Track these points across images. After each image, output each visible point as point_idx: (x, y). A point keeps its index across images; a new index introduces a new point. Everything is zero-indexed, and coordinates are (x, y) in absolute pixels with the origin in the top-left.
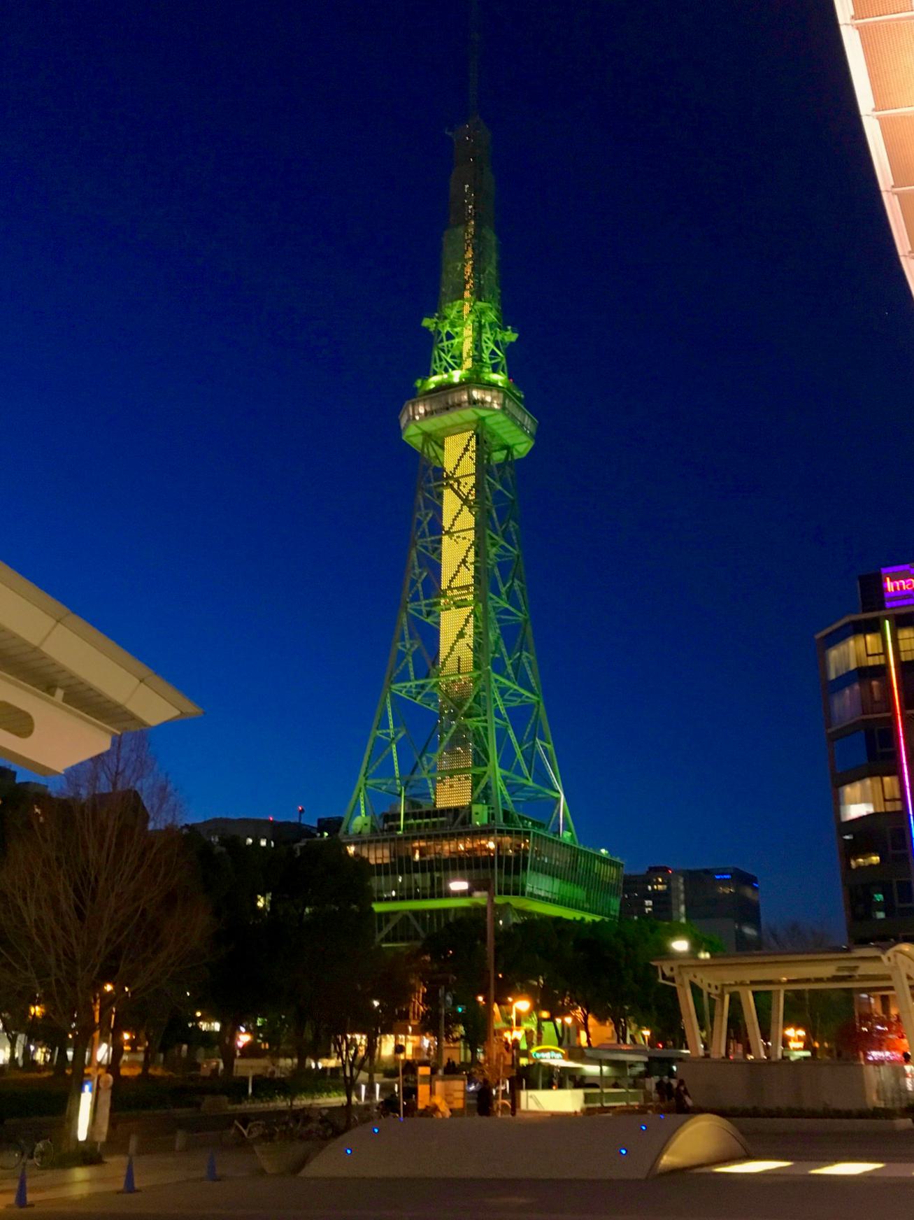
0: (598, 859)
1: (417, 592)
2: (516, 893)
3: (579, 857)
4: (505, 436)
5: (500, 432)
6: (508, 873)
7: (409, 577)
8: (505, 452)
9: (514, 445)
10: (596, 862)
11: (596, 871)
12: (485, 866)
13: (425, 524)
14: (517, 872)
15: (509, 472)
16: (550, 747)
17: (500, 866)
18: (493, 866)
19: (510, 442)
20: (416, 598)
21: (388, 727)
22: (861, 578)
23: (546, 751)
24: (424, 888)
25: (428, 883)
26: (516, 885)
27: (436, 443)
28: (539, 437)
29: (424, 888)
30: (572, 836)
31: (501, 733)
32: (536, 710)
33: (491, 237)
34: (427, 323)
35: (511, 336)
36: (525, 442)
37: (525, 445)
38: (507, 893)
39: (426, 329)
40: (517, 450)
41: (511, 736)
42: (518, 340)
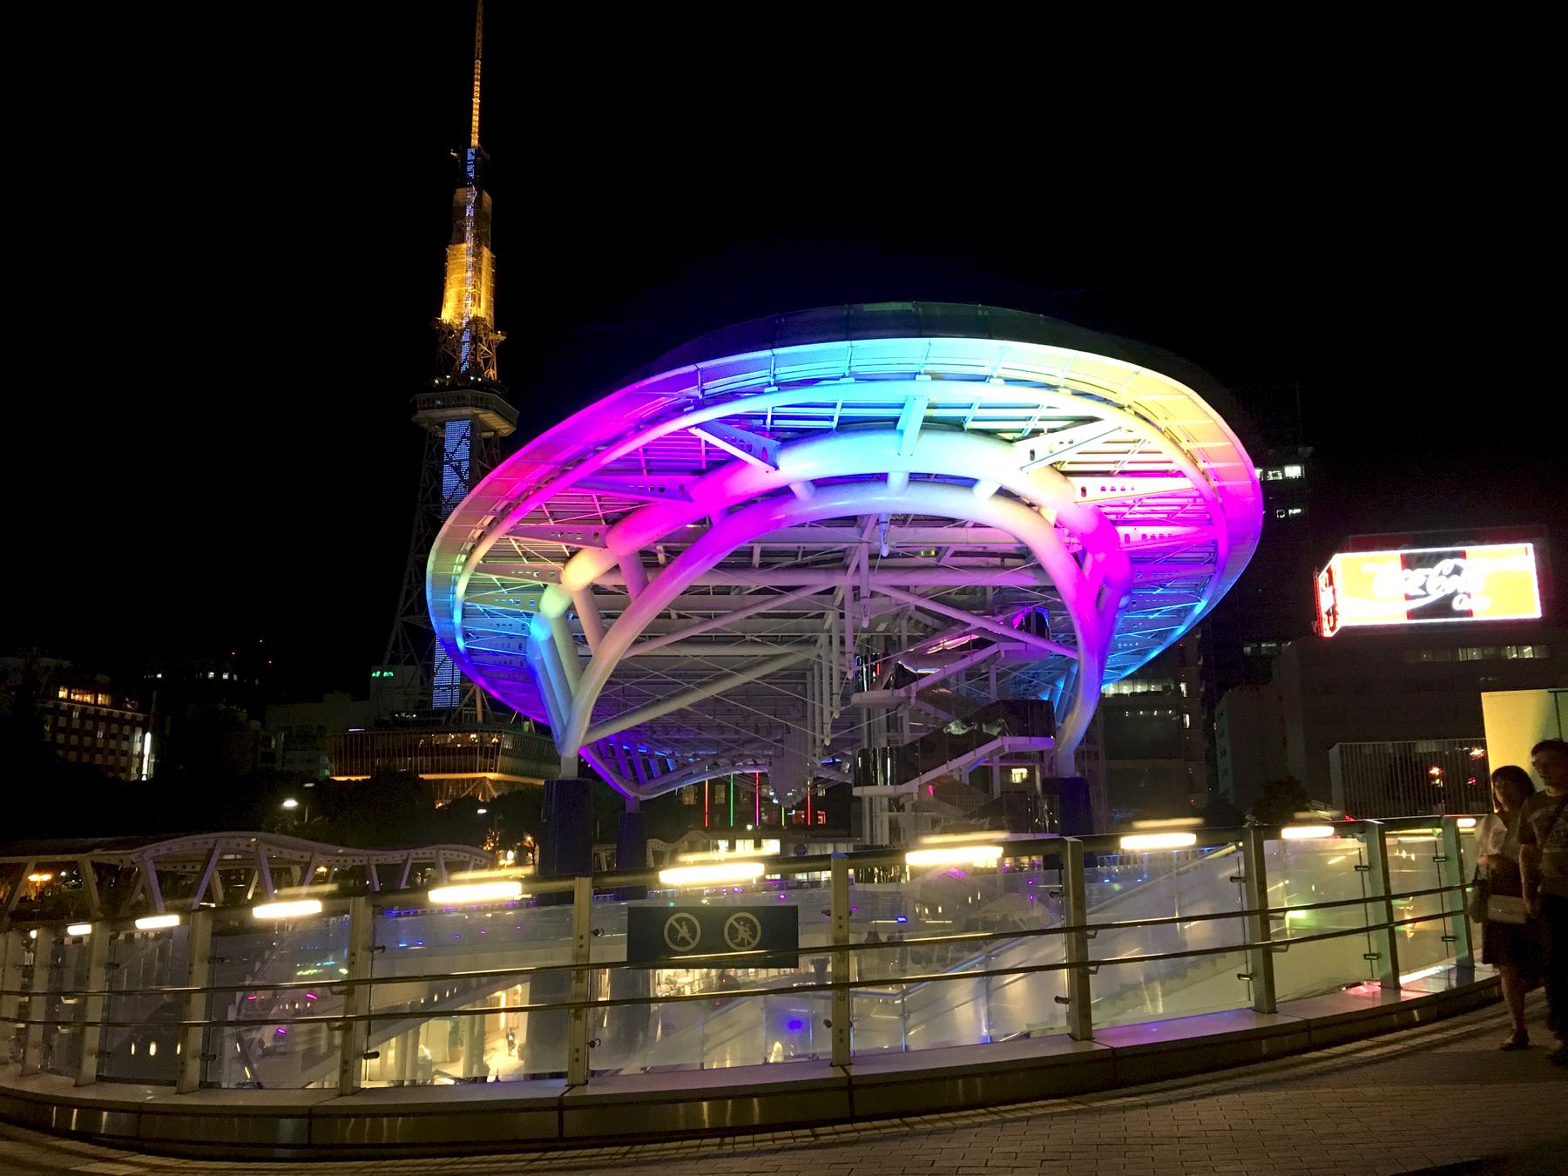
2: (491, 771)
6: (486, 757)
9: (499, 429)
14: (492, 757)
17: (481, 754)
19: (497, 427)
30: (530, 723)
33: (486, 253)
35: (500, 337)
37: (507, 430)
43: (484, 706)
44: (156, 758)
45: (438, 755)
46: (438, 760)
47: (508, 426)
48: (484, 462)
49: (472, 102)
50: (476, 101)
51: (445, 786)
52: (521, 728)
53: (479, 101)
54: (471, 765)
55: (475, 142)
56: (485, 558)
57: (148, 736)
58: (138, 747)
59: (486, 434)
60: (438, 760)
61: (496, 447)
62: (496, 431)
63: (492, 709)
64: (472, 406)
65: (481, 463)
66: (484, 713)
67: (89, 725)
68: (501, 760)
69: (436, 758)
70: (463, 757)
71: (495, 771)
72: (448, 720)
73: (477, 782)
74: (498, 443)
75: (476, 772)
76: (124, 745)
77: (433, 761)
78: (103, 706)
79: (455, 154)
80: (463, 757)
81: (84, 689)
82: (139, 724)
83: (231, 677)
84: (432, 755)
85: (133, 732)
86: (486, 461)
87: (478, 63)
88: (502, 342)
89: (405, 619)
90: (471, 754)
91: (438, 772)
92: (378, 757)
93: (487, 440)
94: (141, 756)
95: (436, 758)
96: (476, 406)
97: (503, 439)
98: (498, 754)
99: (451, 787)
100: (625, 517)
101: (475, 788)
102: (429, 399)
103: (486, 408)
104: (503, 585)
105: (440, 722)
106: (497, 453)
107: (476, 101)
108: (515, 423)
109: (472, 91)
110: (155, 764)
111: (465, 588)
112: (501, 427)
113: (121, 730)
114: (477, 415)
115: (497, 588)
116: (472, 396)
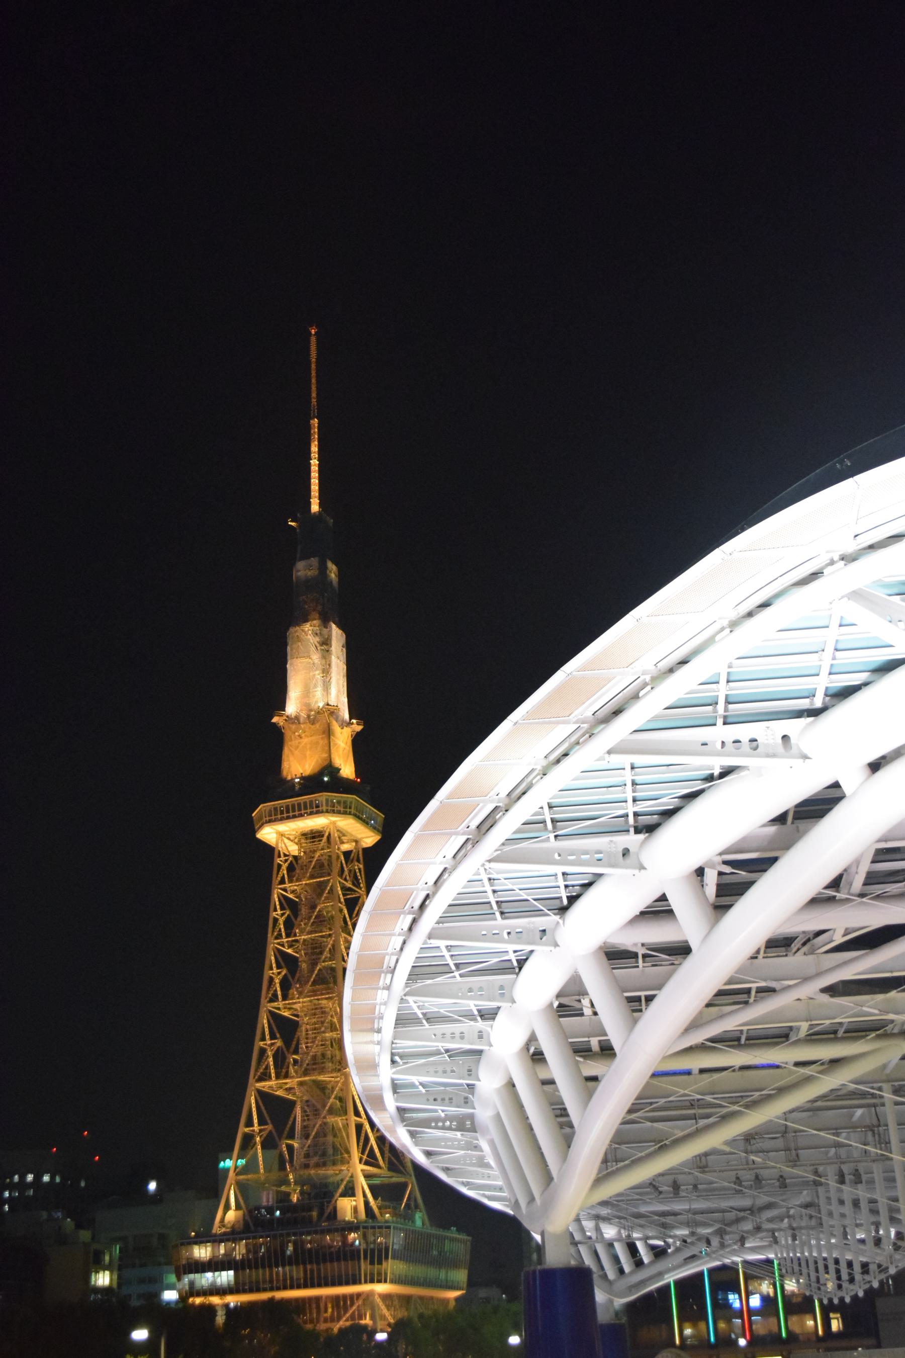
0: (447, 1238)
2: (379, 1281)
3: (432, 1240)
4: (354, 833)
5: (349, 830)
6: (372, 1263)
7: (268, 973)
10: (446, 1241)
11: (446, 1250)
12: (352, 1259)
13: (281, 921)
14: (380, 1263)
17: (365, 1258)
19: (359, 836)
20: (274, 998)
21: (252, 1125)
24: (298, 1279)
25: (302, 1275)
26: (379, 1274)
27: (289, 839)
29: (298, 1279)
30: (423, 1215)
34: (275, 720)
36: (372, 836)
38: (372, 1281)
39: (274, 724)
40: (364, 842)
41: (380, 1158)
42: (362, 730)
43: (365, 1195)
45: (311, 1262)
46: (312, 1271)
47: (372, 834)
48: (345, 880)
49: (310, 463)
50: (314, 462)
51: (322, 1305)
52: (413, 1222)
53: (317, 462)
54: (354, 1275)
55: (315, 507)
56: (442, 920)
59: (346, 847)
60: (312, 1271)
61: (358, 861)
62: (356, 842)
64: (327, 812)
65: (342, 881)
68: (391, 1266)
69: (309, 1267)
70: (343, 1263)
71: (385, 1281)
72: (321, 1214)
73: (363, 1297)
74: (361, 856)
75: (360, 1283)
77: (305, 1271)
79: (293, 524)
80: (343, 1263)
86: (348, 878)
87: (315, 422)
88: (358, 733)
89: (259, 1085)
91: (313, 1286)
93: (347, 854)
95: (309, 1267)
96: (334, 812)
97: (366, 850)
98: (387, 1258)
99: (329, 1305)
100: (666, 820)
102: (276, 809)
103: (345, 813)
104: (458, 966)
105: (308, 1221)
106: (360, 869)
107: (314, 462)
108: (381, 829)
109: (309, 452)
111: (406, 976)
112: (363, 835)
114: (334, 823)
115: (444, 970)
116: (327, 800)
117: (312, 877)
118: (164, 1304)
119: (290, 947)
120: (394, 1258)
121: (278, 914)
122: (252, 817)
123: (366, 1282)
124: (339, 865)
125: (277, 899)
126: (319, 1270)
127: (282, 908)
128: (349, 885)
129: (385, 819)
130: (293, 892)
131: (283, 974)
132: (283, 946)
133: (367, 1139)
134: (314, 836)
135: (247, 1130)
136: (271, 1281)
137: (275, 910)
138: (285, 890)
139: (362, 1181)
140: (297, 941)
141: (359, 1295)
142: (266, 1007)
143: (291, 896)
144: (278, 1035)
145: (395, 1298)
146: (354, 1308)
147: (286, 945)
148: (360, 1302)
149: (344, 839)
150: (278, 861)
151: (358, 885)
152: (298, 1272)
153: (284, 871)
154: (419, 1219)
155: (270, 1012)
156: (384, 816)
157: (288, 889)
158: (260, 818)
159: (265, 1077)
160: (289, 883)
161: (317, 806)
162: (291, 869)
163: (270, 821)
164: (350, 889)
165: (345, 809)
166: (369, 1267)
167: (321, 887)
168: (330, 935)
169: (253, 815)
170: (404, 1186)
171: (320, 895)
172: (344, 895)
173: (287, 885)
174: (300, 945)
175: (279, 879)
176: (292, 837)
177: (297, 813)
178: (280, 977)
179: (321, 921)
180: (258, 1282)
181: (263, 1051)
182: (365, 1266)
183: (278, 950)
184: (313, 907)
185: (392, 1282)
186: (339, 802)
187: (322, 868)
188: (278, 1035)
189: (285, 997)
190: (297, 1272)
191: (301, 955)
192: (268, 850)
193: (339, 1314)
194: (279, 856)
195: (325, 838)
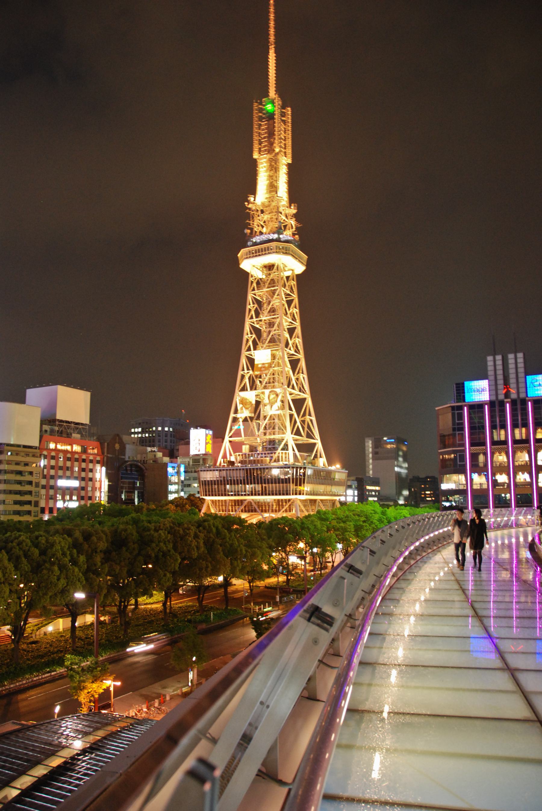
1: (250, 346)
2: (300, 494)
6: (296, 485)
8: (291, 272)
15: (293, 283)
16: (314, 419)
17: (293, 483)
18: (289, 483)
22: (456, 384)
23: (311, 421)
25: (260, 489)
26: (300, 491)
28: (309, 265)
29: (259, 491)
31: (291, 416)
32: (307, 401)
38: (296, 494)
43: (294, 450)
44: (109, 482)
45: (265, 483)
54: (287, 491)
57: (104, 469)
58: (98, 476)
60: (265, 487)
61: (293, 280)
62: (293, 270)
63: (299, 451)
66: (295, 455)
67: (69, 464)
68: (307, 488)
69: (264, 485)
71: (303, 494)
73: (292, 501)
76: (90, 475)
78: (77, 453)
81: (62, 443)
82: (98, 462)
83: (169, 429)
84: (261, 483)
85: (94, 466)
90: (286, 483)
92: (228, 484)
94: (100, 481)
95: (264, 485)
98: (304, 483)
101: (290, 505)
102: (250, 252)
108: (305, 264)
110: (109, 485)
113: (87, 466)
116: (276, 246)
117: (268, 288)
118: (75, 600)
119: (258, 324)
120: (308, 483)
121: (251, 306)
122: (237, 257)
123: (293, 494)
124: (283, 281)
125: (250, 299)
126: (269, 487)
127: (253, 303)
128: (288, 292)
129: (308, 259)
130: (259, 296)
131: (253, 338)
132: (254, 323)
133: (295, 422)
134: (270, 267)
135: (234, 415)
136: (245, 491)
137: (250, 304)
138: (255, 295)
139: (291, 444)
140: (261, 321)
141: (289, 500)
142: (244, 353)
143: (259, 298)
144: (250, 368)
145: (309, 501)
146: (287, 506)
147: (255, 323)
148: (290, 503)
149: (286, 268)
150: (251, 279)
151: (293, 292)
152: (258, 487)
153: (255, 284)
154: (322, 462)
155: (247, 357)
156: (307, 257)
157: (257, 294)
158: (242, 257)
159: (244, 389)
160: (258, 290)
161: (271, 249)
162: (258, 283)
163: (247, 258)
164: (289, 295)
165: (286, 252)
166: (295, 487)
167: (274, 292)
168: (278, 317)
169: (239, 255)
170: (314, 444)
171: (272, 297)
172: (286, 298)
173: (256, 291)
174: (263, 323)
175: (252, 288)
176: (259, 268)
177: (260, 253)
178: (252, 339)
179: (273, 311)
180: (238, 491)
181: (243, 377)
182: (292, 486)
183: (251, 325)
184: (269, 302)
185: (307, 494)
186: (283, 248)
187: (273, 283)
188: (250, 368)
189: (255, 349)
190: (258, 487)
191: (263, 328)
192: (246, 275)
193: (279, 508)
194: (252, 277)
195: (275, 267)
